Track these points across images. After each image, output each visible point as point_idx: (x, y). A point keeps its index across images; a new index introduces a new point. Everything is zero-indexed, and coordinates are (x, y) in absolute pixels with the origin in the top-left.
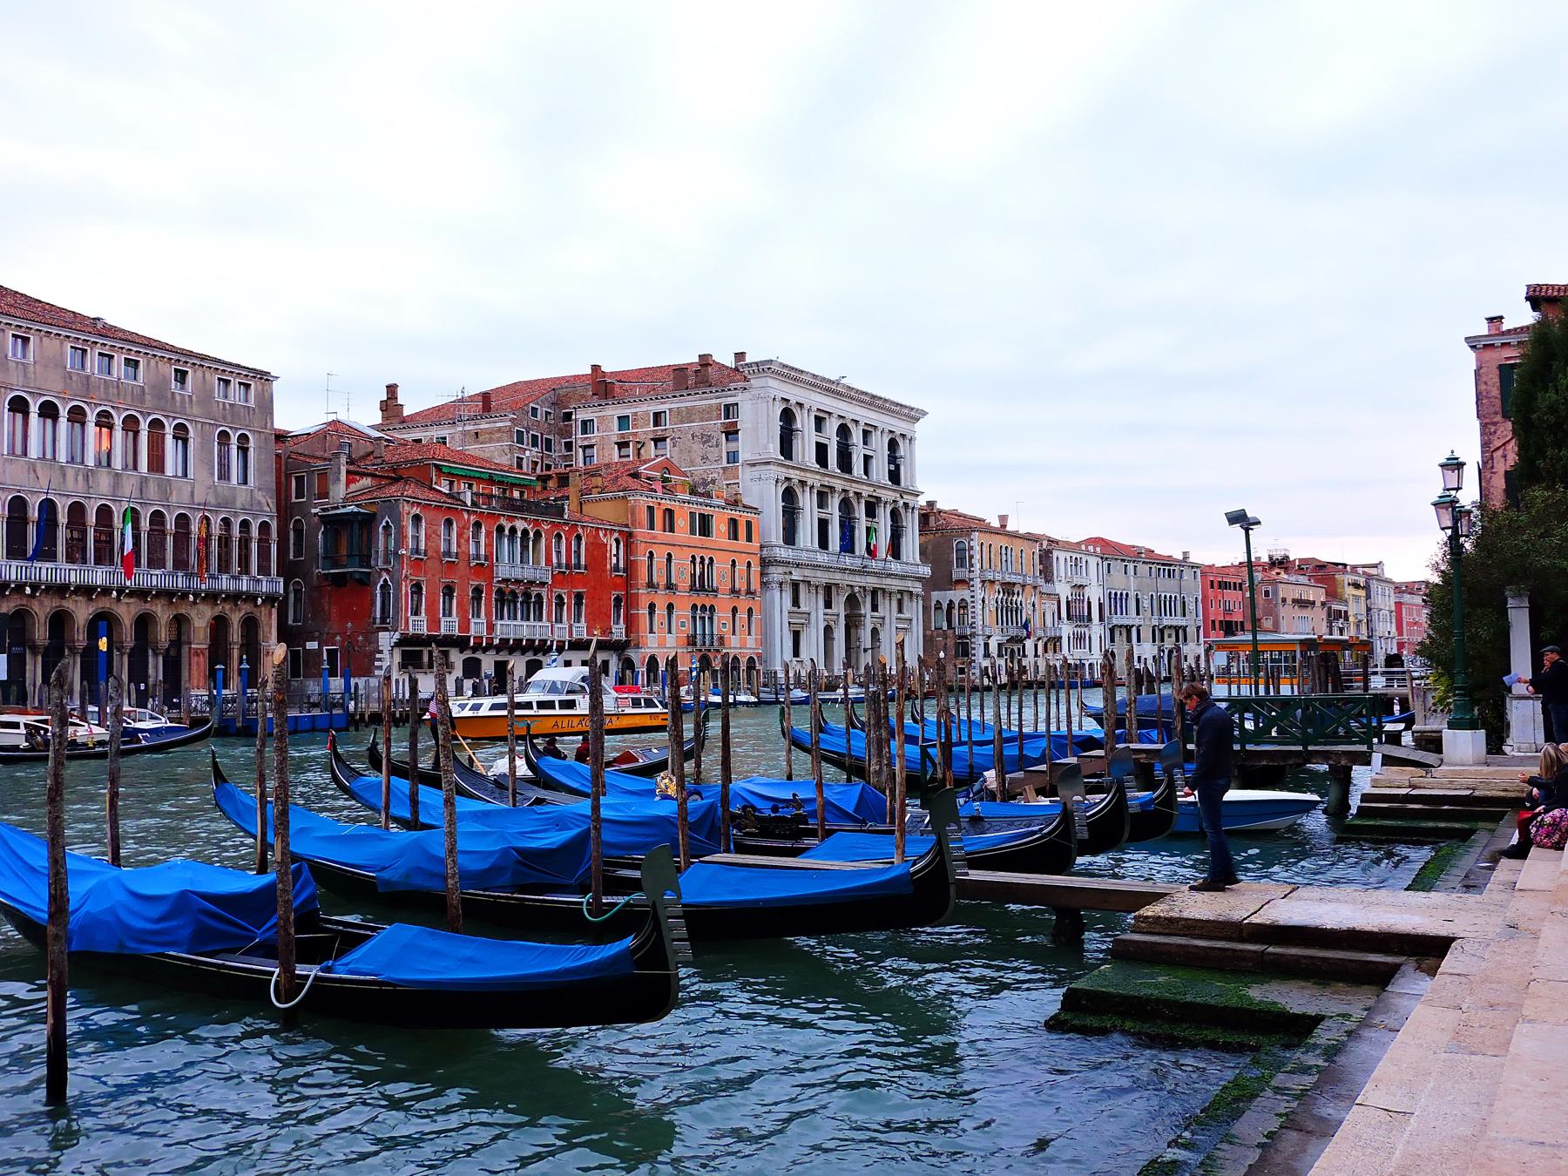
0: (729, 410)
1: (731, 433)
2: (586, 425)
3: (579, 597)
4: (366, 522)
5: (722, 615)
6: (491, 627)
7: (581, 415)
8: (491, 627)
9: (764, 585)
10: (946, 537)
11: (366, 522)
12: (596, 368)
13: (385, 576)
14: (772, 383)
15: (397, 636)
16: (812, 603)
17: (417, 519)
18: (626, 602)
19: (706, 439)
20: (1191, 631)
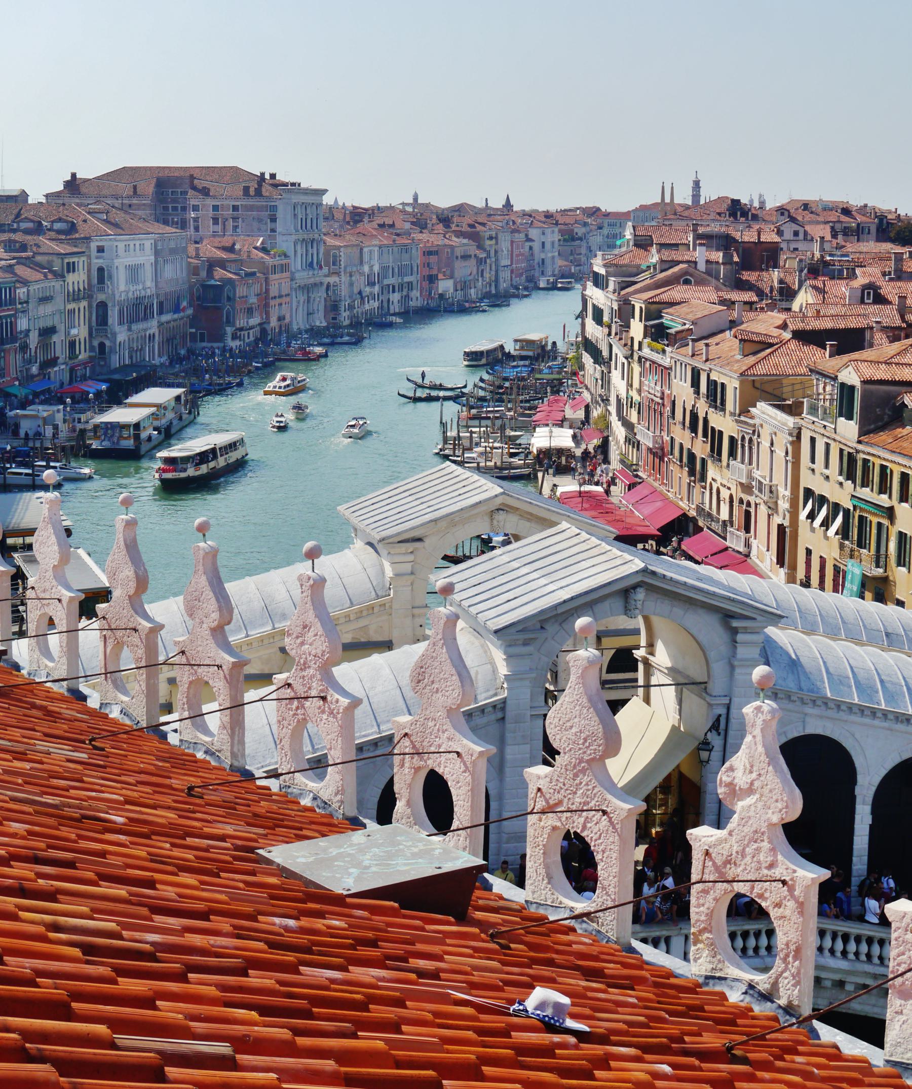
1: (273, 219)
16: (300, 294)
18: (267, 305)
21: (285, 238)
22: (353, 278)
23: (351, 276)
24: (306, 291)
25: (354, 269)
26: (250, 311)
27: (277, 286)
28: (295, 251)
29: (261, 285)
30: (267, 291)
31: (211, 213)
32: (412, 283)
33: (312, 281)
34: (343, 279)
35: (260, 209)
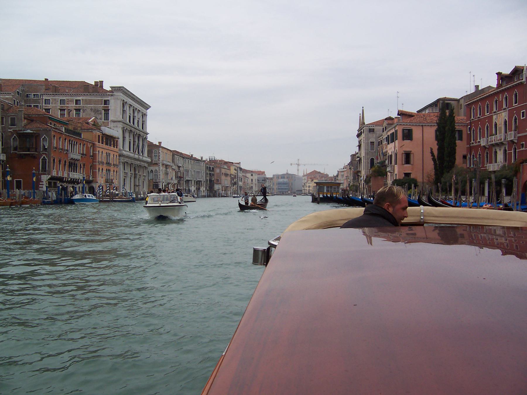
0: (106, 102)
1: (107, 111)
2: (47, 101)
3: (84, 165)
4: (36, 136)
5: (112, 172)
6: (68, 175)
7: (45, 97)
8: (68, 175)
9: (119, 162)
10: (154, 148)
11: (36, 136)
12: (46, 80)
13: (44, 155)
14: (121, 94)
15: (50, 176)
16: (128, 170)
17: (54, 136)
18: (93, 167)
19: (96, 111)
20: (203, 182)
21: (115, 124)
22: (168, 170)
23: (166, 168)
24: (133, 169)
25: (169, 164)
26: (73, 165)
27: (104, 154)
28: (124, 138)
29: (87, 147)
30: (94, 156)
31: (59, 105)
32: (201, 181)
33: (138, 163)
34: (161, 168)
35: (96, 102)
